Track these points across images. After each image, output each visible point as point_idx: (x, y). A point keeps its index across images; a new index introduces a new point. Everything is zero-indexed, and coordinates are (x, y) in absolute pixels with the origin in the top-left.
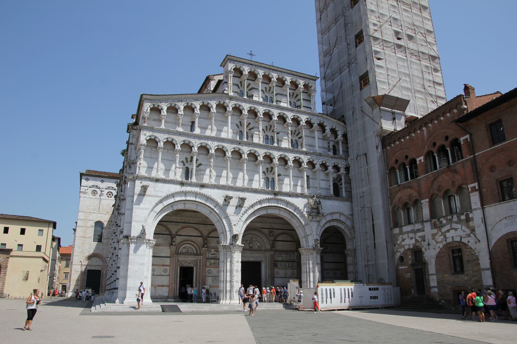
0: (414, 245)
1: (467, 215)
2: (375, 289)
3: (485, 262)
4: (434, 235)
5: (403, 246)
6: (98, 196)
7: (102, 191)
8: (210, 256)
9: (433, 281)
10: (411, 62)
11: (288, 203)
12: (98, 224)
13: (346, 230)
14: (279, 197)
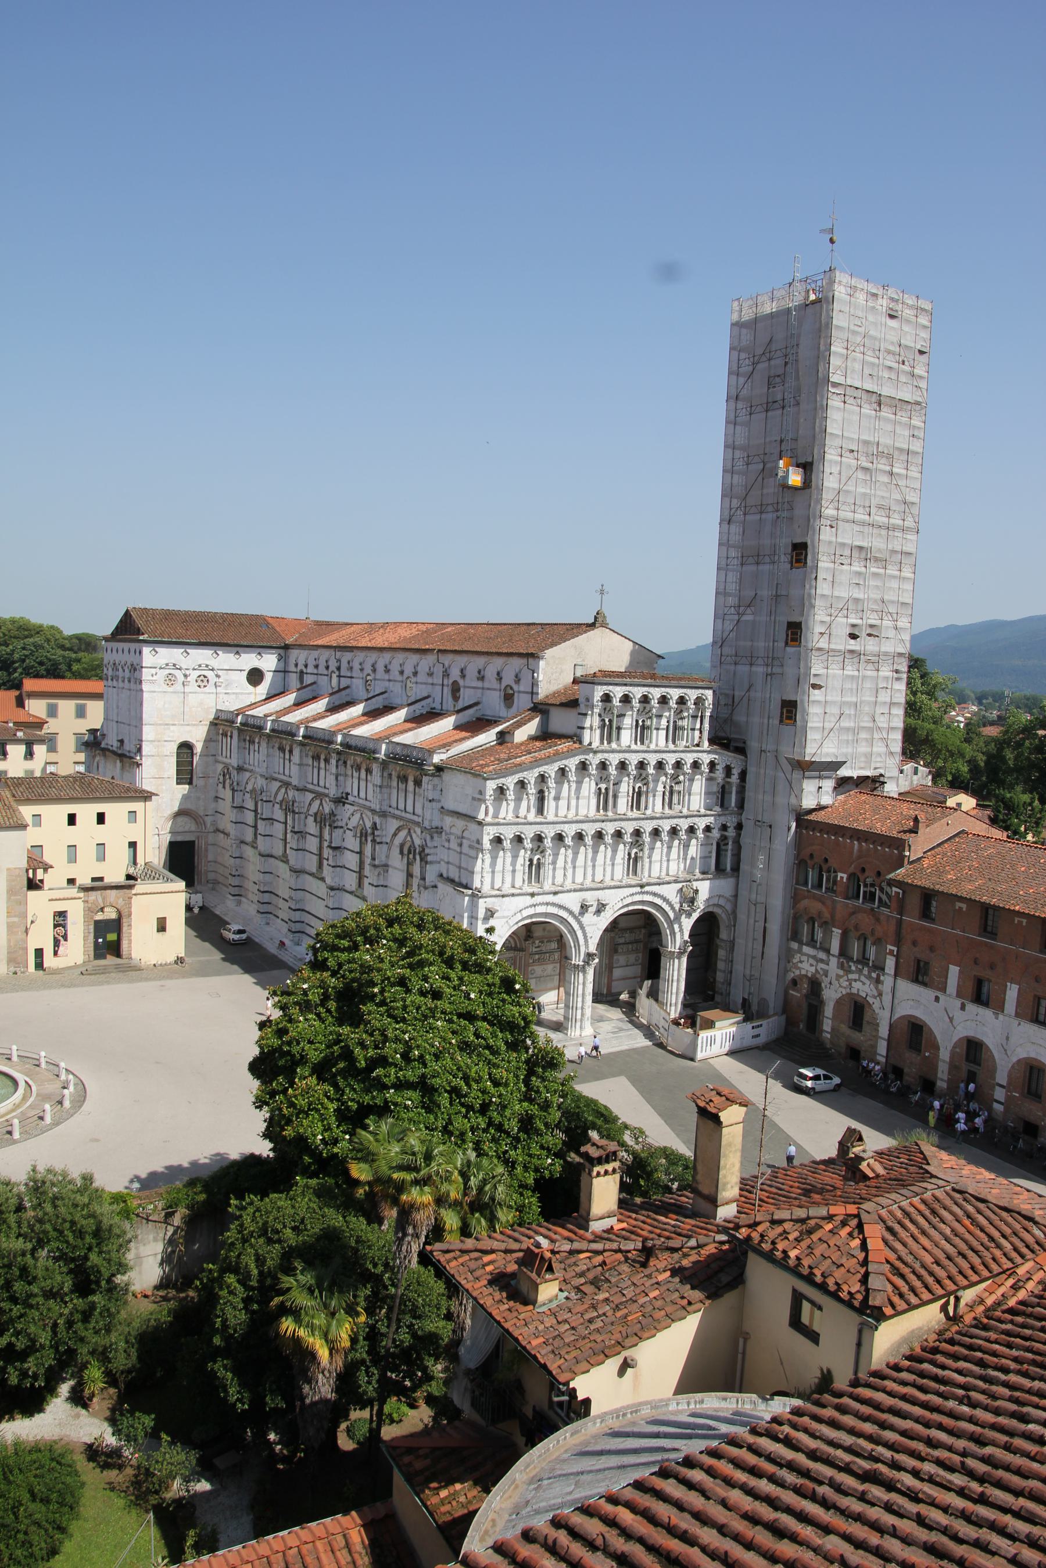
0: (814, 975)
1: (878, 976)
2: (758, 1026)
3: (884, 1031)
4: (838, 977)
5: (799, 968)
6: (178, 687)
7: (186, 676)
8: (535, 950)
9: (827, 1025)
10: (864, 677)
11: (655, 894)
12: (186, 747)
13: (723, 916)
14: (647, 889)
